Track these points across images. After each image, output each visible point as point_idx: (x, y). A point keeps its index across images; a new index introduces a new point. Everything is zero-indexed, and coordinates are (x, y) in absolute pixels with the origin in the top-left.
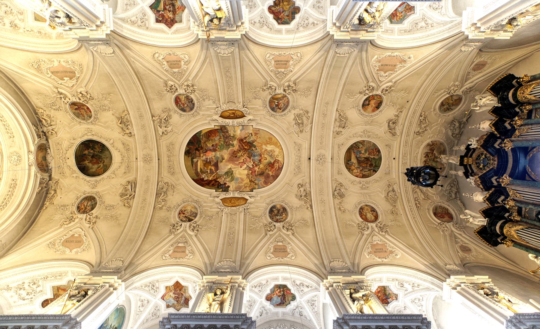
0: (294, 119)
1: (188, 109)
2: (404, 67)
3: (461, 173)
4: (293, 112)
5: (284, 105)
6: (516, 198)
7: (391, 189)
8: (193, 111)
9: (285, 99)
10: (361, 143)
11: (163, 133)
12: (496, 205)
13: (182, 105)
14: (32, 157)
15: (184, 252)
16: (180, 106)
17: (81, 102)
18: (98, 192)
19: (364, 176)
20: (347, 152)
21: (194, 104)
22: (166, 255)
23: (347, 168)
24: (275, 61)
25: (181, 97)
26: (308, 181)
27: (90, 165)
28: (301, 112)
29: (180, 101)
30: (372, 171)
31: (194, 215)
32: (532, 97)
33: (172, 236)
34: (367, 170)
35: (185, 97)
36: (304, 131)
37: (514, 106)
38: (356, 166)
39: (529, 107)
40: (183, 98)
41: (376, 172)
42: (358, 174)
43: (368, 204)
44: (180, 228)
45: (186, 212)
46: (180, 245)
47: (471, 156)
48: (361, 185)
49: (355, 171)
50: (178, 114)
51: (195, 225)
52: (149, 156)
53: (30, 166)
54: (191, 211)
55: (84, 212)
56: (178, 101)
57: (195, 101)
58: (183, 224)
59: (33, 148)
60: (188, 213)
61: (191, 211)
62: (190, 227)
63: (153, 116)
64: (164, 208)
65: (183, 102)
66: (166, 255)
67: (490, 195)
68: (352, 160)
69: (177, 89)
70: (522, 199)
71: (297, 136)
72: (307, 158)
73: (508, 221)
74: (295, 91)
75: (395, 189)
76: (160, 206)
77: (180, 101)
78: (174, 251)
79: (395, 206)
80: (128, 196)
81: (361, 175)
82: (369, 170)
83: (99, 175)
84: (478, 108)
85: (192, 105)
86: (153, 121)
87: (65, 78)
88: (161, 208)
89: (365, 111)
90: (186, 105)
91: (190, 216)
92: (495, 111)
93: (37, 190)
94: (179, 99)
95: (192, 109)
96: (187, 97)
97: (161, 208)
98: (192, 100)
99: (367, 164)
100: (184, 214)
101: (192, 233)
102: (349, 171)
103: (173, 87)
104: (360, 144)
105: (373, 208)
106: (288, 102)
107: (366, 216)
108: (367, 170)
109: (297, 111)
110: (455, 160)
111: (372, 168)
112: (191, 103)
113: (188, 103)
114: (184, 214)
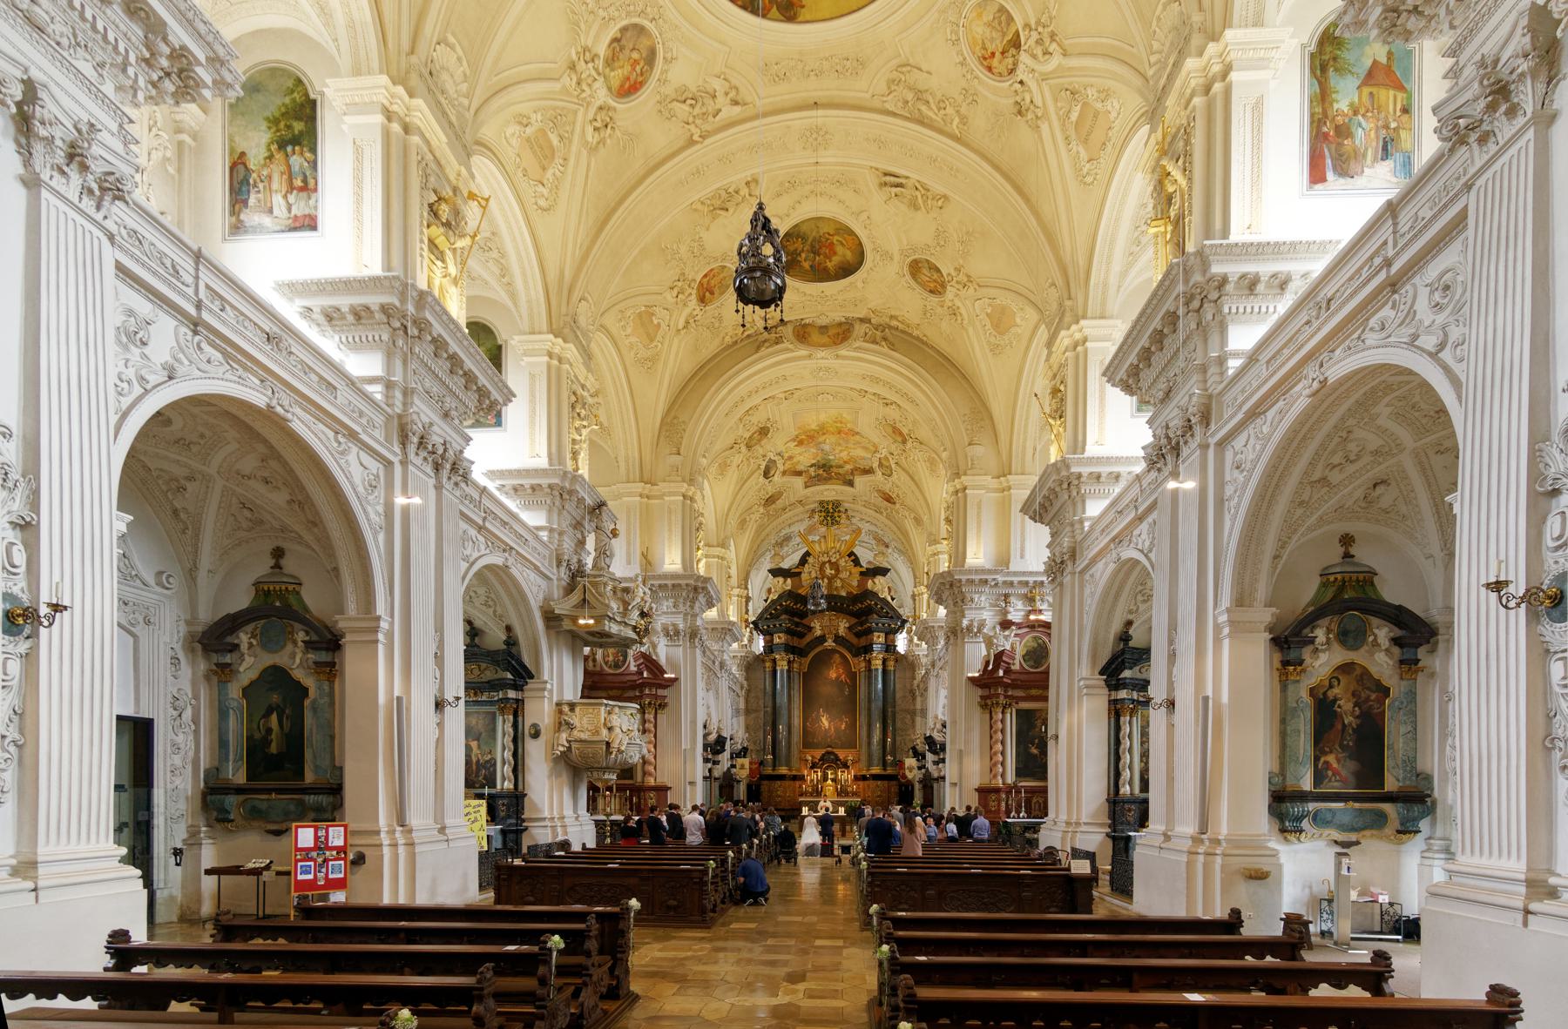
1: (644, 43)
8: (646, 23)
11: (735, 103)
13: (638, 69)
14: (821, 353)
15: (1096, 115)
16: (642, 74)
17: (694, 292)
18: (902, 251)
21: (624, 30)
22: (1085, 170)
25: (616, 83)
27: (836, 259)
29: (628, 79)
31: (1003, 18)
33: (1045, 127)
35: (613, 70)
40: (617, 76)
44: (1030, 91)
45: (988, 45)
46: (1074, 116)
50: (666, 71)
51: (1035, 36)
52: (808, 134)
53: (838, 356)
54: (989, 25)
55: (943, 286)
56: (630, 87)
57: (613, 31)
58: (1021, 74)
59: (803, 352)
60: (992, 40)
61: (989, 25)
62: (1034, 57)
63: (691, 142)
64: (963, 110)
65: (628, 68)
66: (1085, 170)
69: (601, 108)
76: (957, 120)
77: (628, 79)
78: (1086, 141)
80: (917, 193)
83: (860, 244)
85: (629, 34)
86: (703, 137)
87: (655, 322)
88: (964, 120)
90: (635, 55)
91: (1004, 34)
93: (886, 350)
94: (622, 86)
95: (640, 30)
96: (611, 61)
97: (964, 120)
98: (616, 40)
100: (993, 54)
101: (1056, 61)
103: (598, 124)
112: (623, 42)
113: (627, 52)
114: (993, 54)
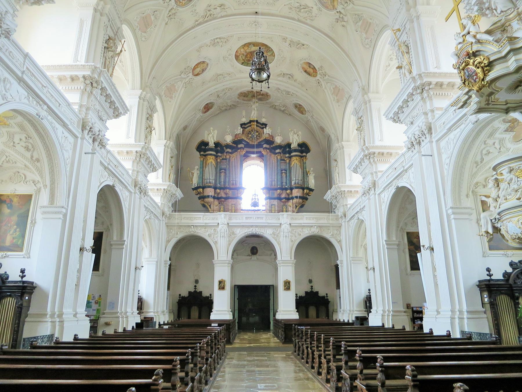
0: (306, 5)
2: (334, 100)
3: (244, 120)
4: (315, 8)
5: (325, 2)
6: (231, 158)
7: (226, 76)
9: (331, 6)
10: (272, 54)
12: (224, 148)
19: (237, 57)
20: (264, 44)
23: (245, 44)
24: (370, 23)
26: (229, 12)
28: (314, 14)
30: (243, 61)
32: (293, 163)
34: (243, 58)
36: (290, 11)
37: (290, 154)
38: (248, 51)
39: (288, 161)
41: (242, 64)
42: (240, 52)
43: (209, 66)
47: (257, 126)
48: (228, 56)
49: (242, 50)
67: (231, 145)
68: (254, 47)
70: (231, 160)
71: (285, 4)
72: (257, 10)
73: (216, 157)
74: (337, 20)
75: (225, 78)
79: (210, 82)
81: (238, 55)
82: (243, 60)
84: (292, 134)
89: (304, 63)
92: (289, 145)
99: (250, 58)
102: (242, 46)
104: (270, 54)
105: (206, 69)
106: (327, 8)
107: (197, 67)
108: (243, 58)
109: (315, 11)
110: (254, 116)
111: (246, 61)
